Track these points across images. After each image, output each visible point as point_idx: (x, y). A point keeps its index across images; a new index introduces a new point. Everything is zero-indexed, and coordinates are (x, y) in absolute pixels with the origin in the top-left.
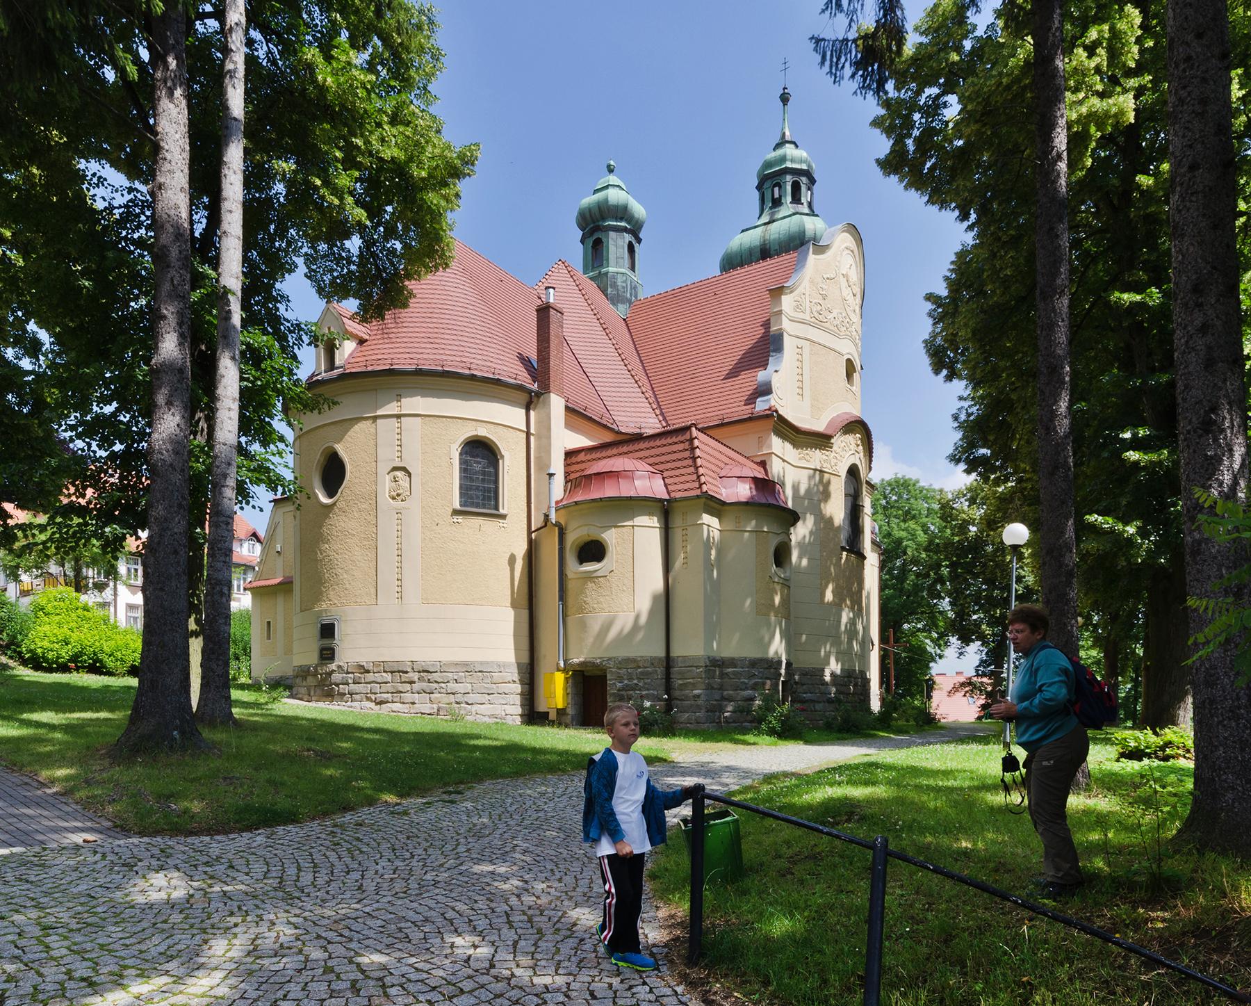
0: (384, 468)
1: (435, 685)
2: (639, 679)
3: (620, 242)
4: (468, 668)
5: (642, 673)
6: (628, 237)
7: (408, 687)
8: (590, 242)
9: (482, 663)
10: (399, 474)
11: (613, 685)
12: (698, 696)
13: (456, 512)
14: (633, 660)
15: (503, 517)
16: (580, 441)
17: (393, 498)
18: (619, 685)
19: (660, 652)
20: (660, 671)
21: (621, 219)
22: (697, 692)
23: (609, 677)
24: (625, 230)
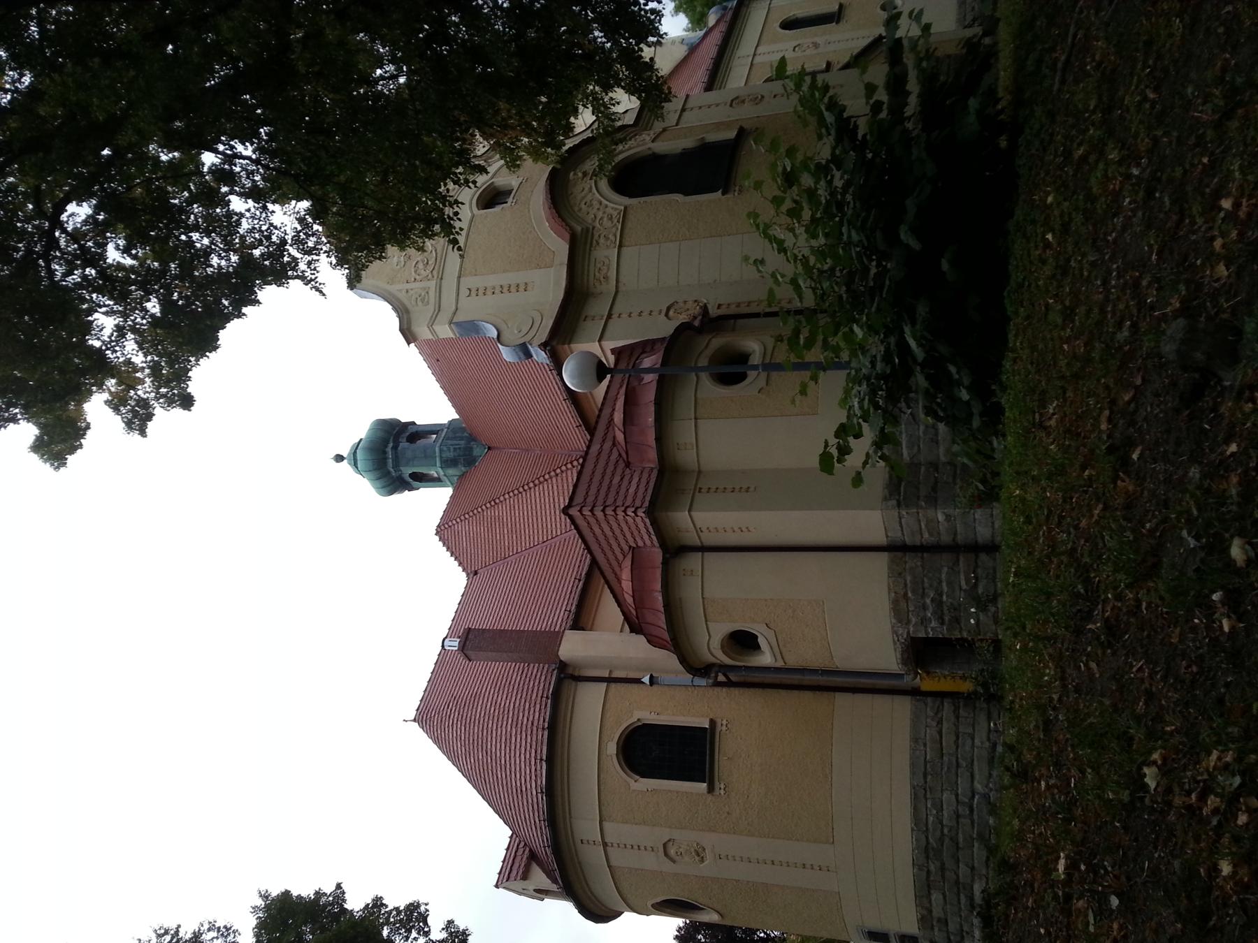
0: (668, 866)
1: (947, 840)
2: (924, 595)
3: (409, 454)
4: (920, 794)
5: (913, 592)
6: (404, 444)
7: (950, 875)
8: (415, 484)
9: (913, 773)
10: (672, 852)
11: (934, 629)
12: (948, 517)
13: (711, 789)
14: (895, 604)
15: (713, 722)
16: (609, 612)
17: (702, 860)
18: (933, 624)
19: (882, 559)
20: (912, 561)
21: (385, 453)
22: (941, 517)
23: (922, 635)
24: (395, 448)
